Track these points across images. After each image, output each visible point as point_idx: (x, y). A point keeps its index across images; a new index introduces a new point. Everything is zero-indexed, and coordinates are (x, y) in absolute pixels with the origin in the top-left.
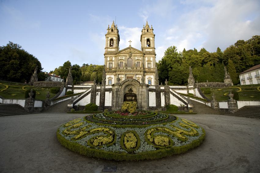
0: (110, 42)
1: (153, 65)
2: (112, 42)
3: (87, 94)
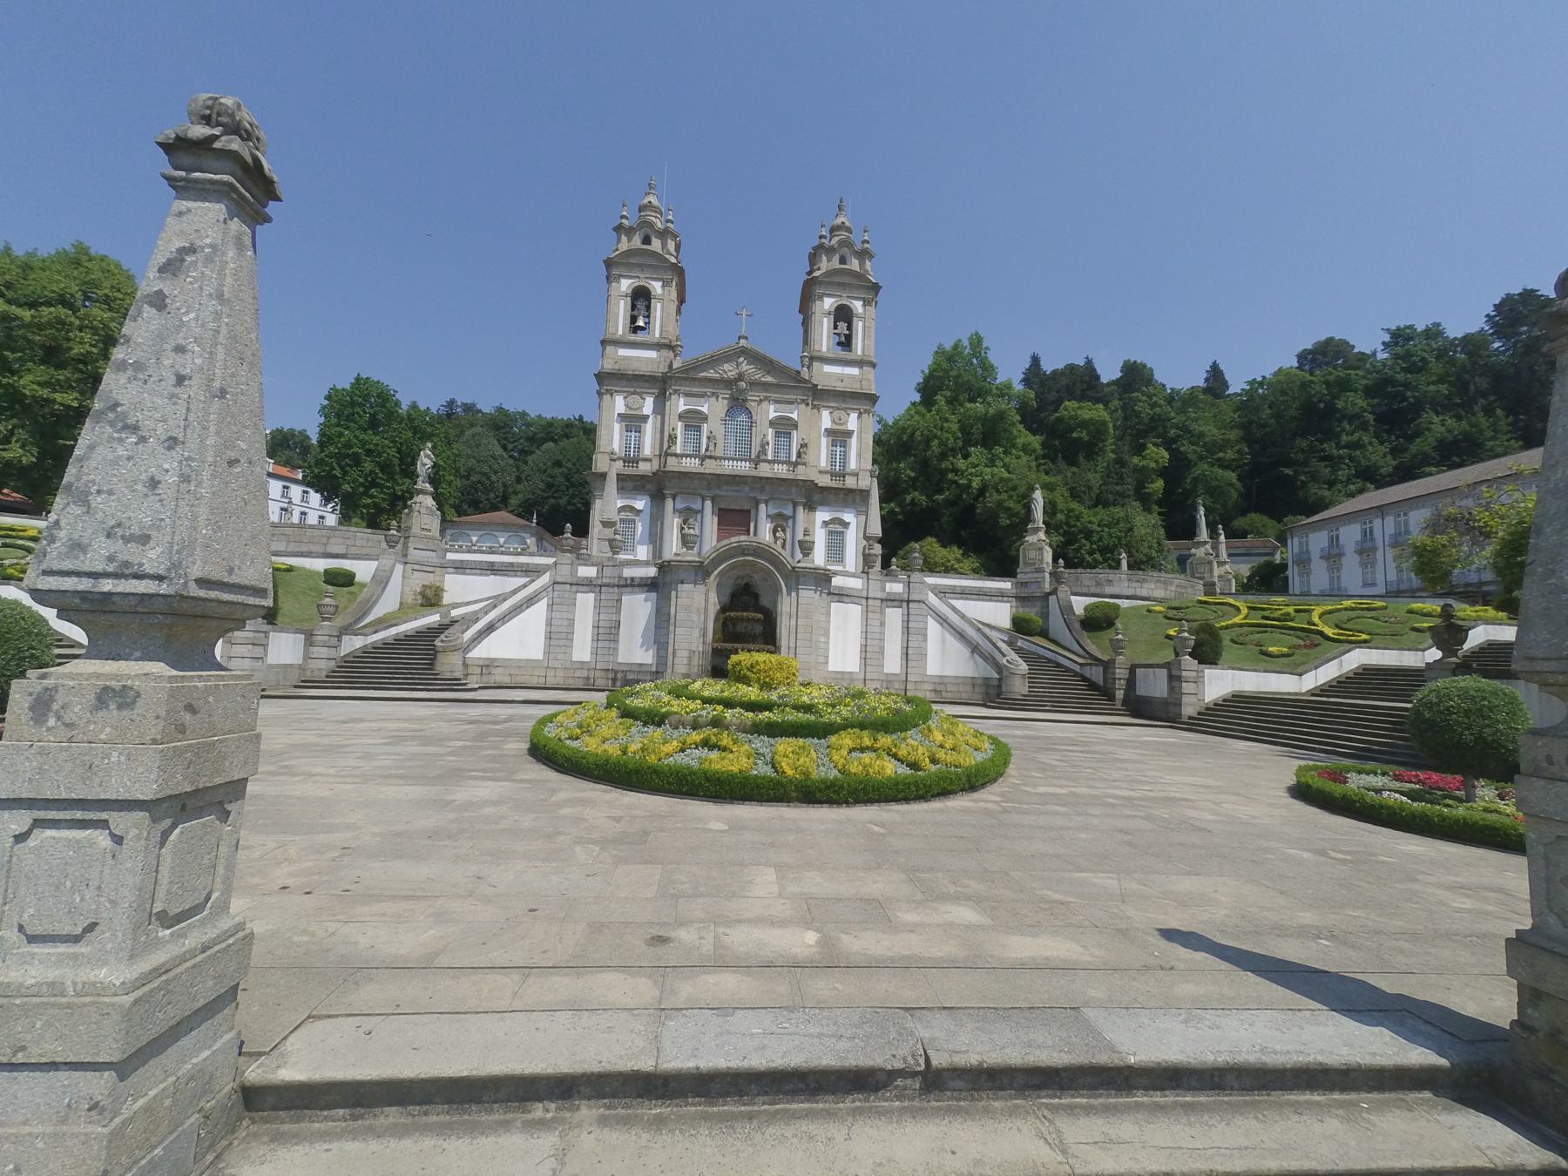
0: (633, 307)
1: (859, 455)
2: (641, 305)
3: (530, 601)
